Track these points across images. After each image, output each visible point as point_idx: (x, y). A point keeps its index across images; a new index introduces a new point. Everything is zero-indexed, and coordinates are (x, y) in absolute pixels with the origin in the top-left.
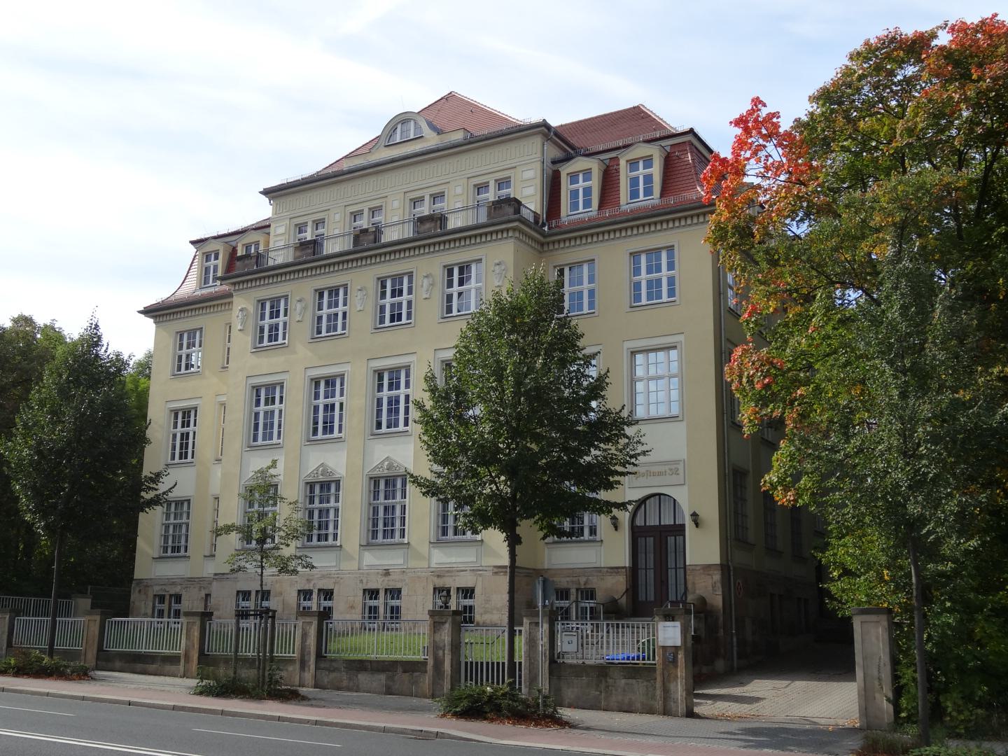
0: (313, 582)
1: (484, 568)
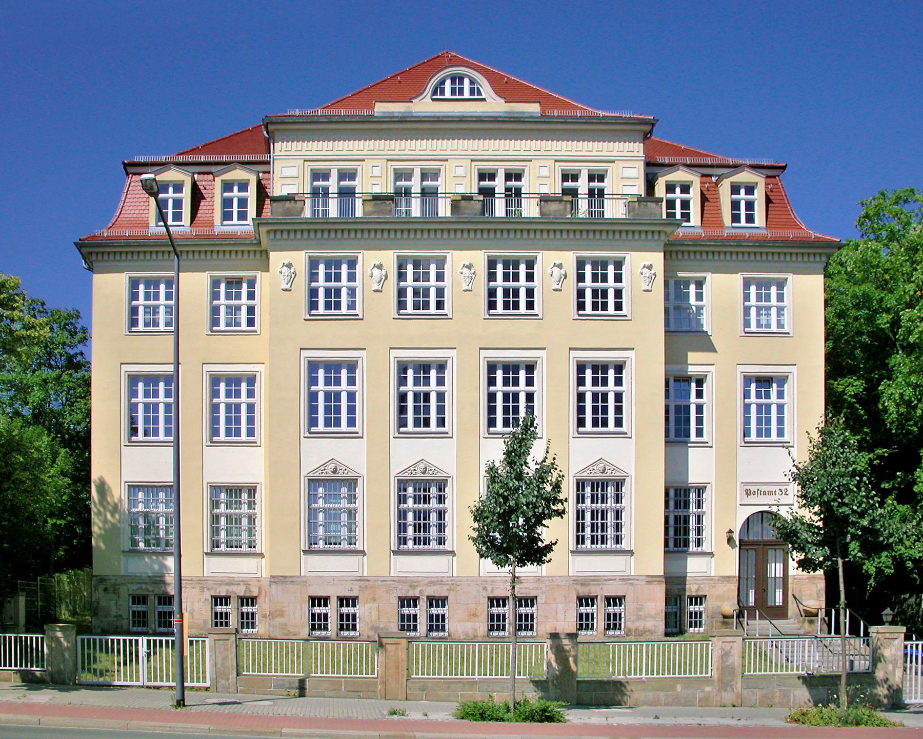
0: (419, 589)
1: (637, 578)
